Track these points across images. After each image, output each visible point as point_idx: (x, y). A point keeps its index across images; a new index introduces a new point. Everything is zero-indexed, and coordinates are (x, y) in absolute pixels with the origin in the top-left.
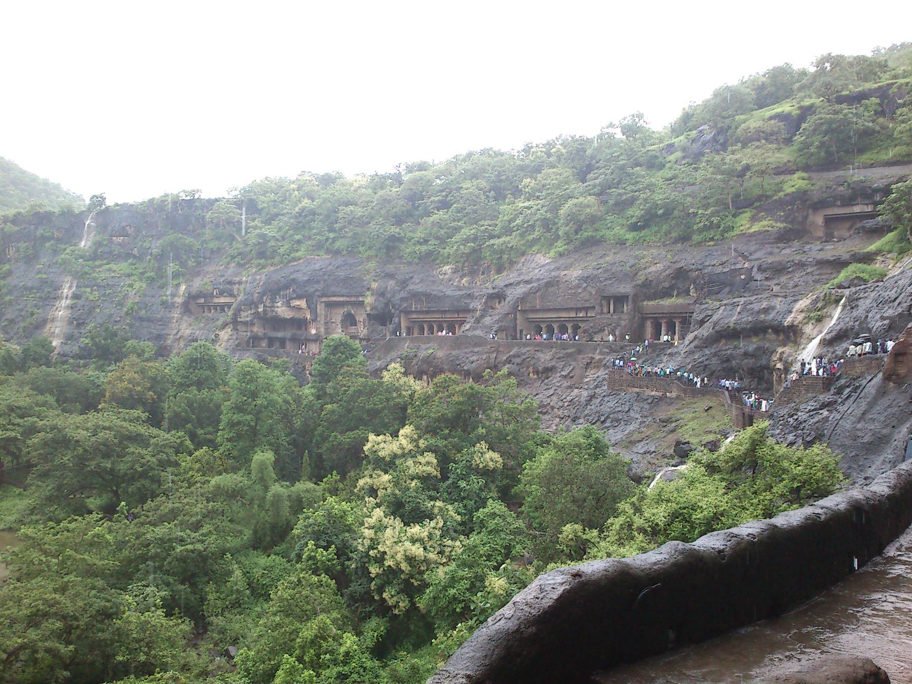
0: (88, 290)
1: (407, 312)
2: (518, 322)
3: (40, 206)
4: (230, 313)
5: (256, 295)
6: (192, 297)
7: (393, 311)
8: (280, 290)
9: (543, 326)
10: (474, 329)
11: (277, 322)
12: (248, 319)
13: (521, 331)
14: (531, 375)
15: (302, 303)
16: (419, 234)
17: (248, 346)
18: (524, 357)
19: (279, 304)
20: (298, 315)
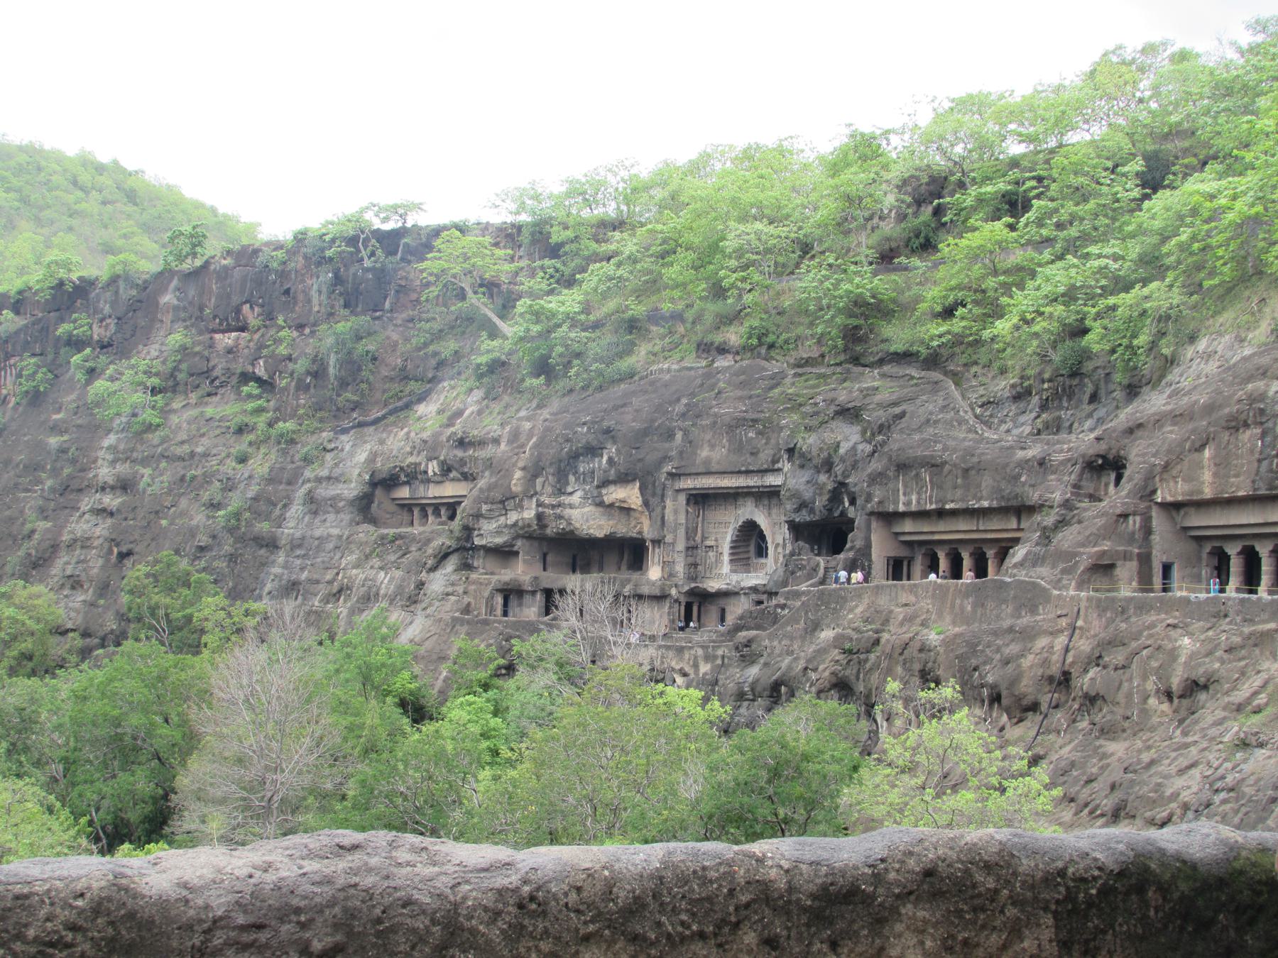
0: (147, 472)
1: (889, 518)
2: (1156, 538)
3: (67, 265)
4: (456, 524)
5: (518, 474)
6: (385, 482)
7: (851, 512)
8: (575, 456)
9: (1233, 550)
10: (1033, 561)
11: (579, 552)
12: (499, 540)
13: (1167, 569)
14: (1153, 701)
15: (630, 495)
16: (933, 295)
17: (491, 610)
18: (1134, 645)
19: (576, 498)
20: (623, 529)
